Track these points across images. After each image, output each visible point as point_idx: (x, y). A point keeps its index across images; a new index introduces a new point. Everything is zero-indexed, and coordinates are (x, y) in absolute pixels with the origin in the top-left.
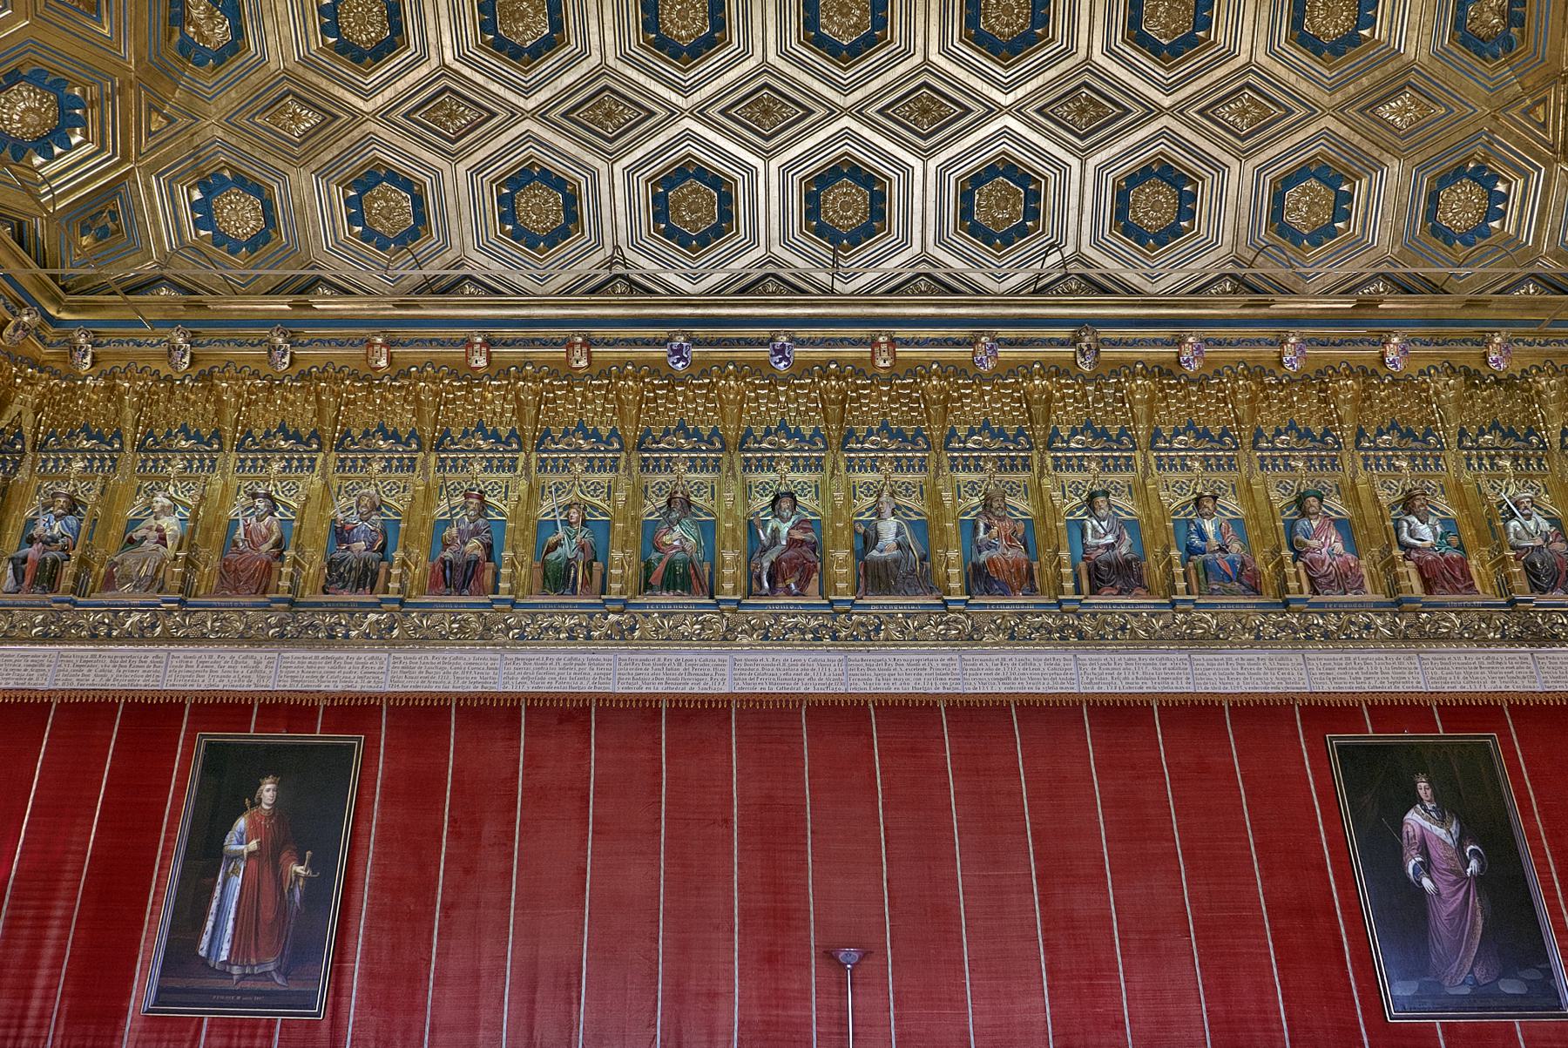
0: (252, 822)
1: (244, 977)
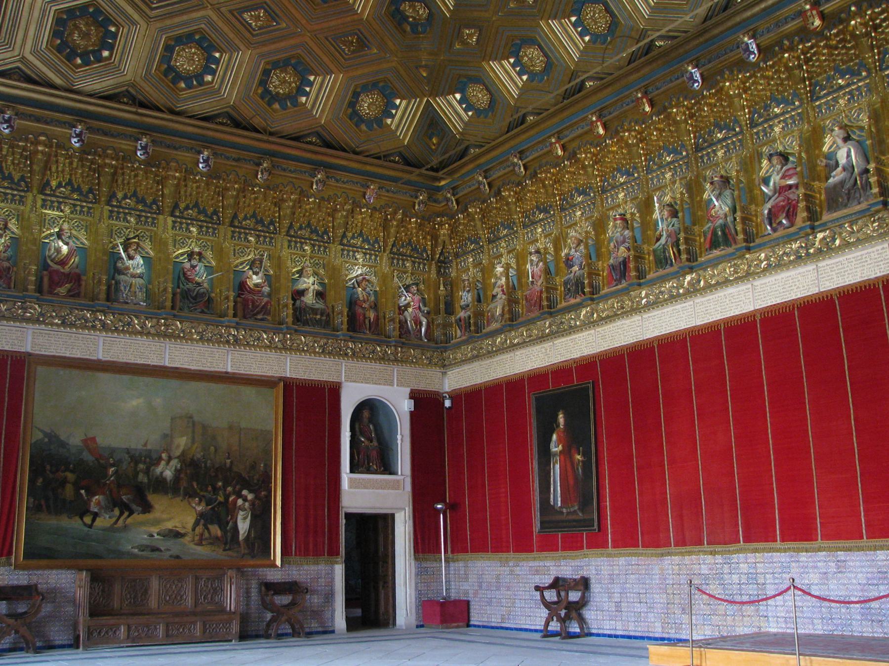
0: (558, 436)
1: (568, 513)
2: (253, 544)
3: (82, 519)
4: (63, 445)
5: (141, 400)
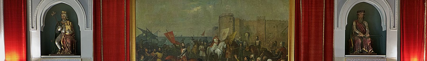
4: (154, 37)
5: (199, 8)
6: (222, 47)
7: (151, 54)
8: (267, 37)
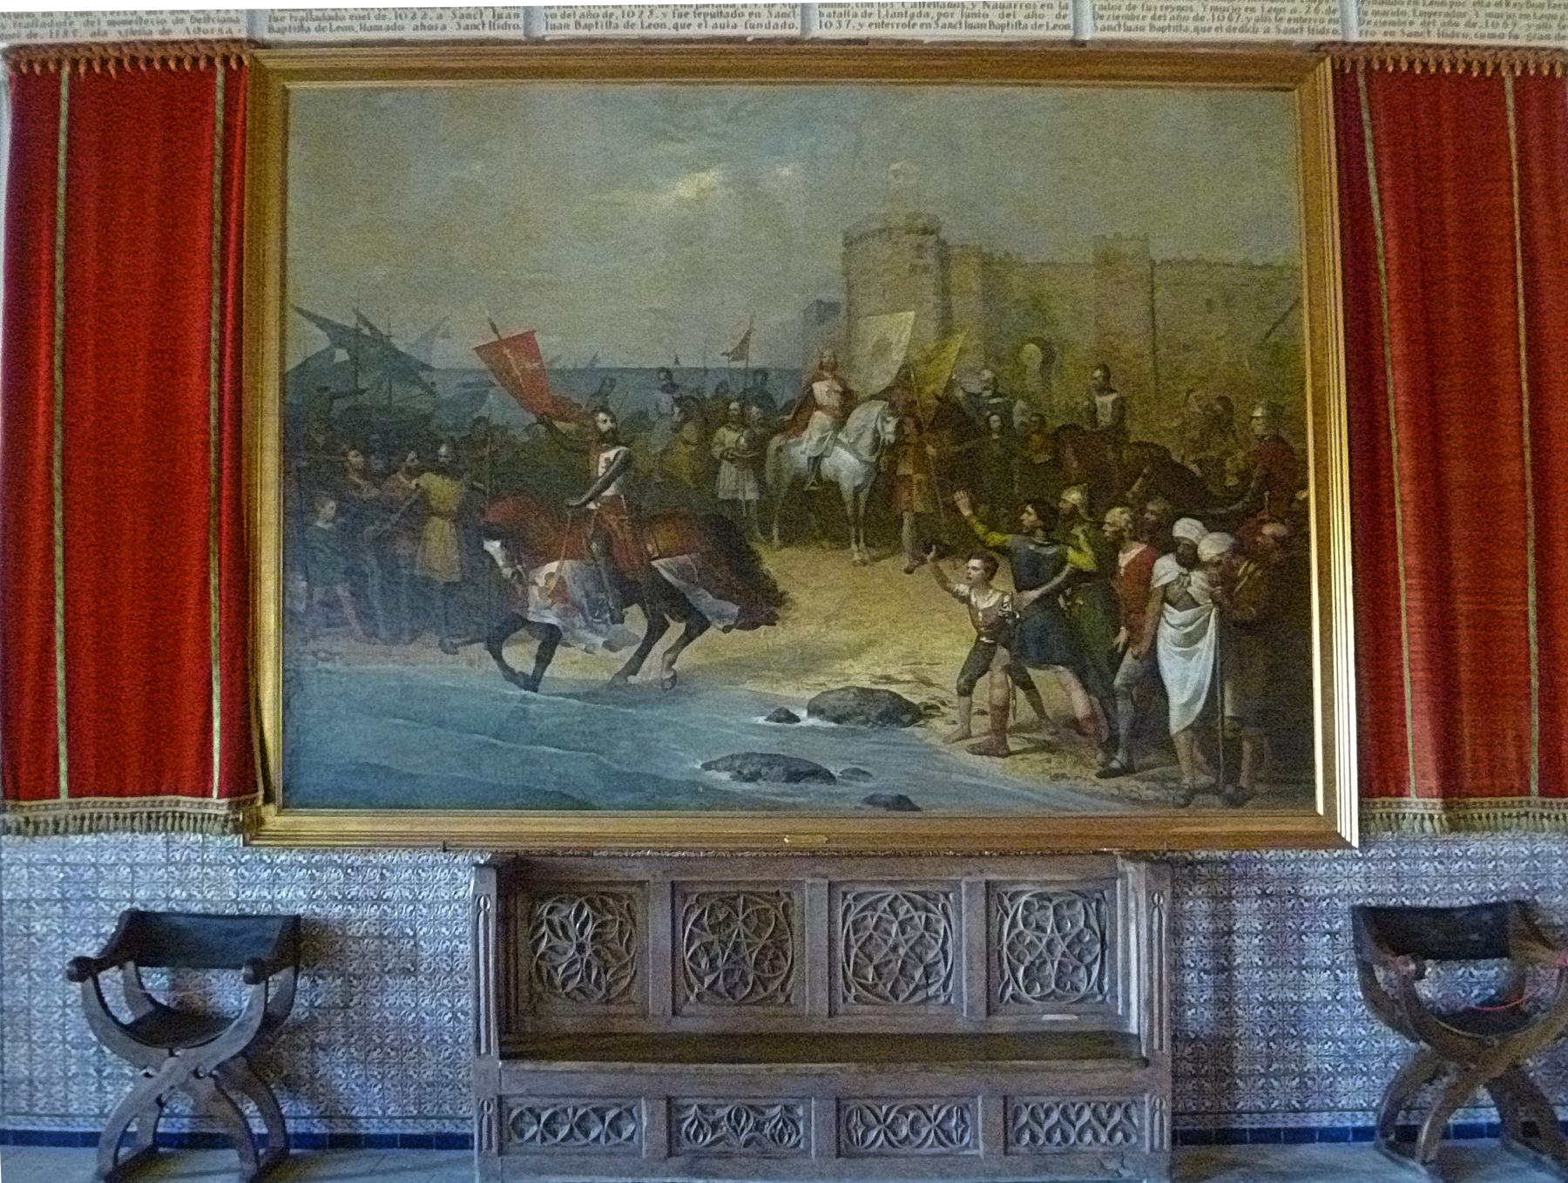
2: (1233, 747)
3: (498, 657)
4: (409, 370)
6: (867, 440)
7: (390, 484)
8: (1163, 372)
